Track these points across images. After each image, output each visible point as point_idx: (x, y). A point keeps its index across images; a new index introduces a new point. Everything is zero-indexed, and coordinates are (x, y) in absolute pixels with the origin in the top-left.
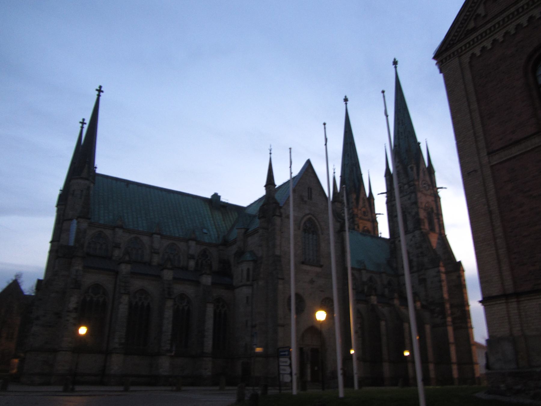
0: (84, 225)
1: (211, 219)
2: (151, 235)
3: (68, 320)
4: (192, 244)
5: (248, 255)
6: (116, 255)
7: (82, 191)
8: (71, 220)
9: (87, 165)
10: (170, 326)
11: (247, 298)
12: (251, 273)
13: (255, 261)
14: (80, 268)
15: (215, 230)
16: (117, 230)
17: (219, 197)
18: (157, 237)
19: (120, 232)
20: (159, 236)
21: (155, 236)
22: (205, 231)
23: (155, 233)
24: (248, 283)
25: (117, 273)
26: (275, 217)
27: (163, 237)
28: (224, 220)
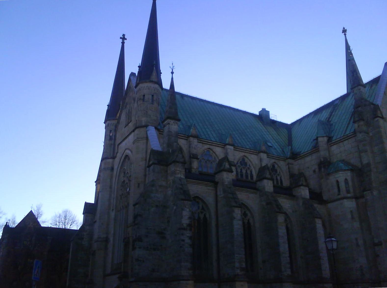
0: (174, 127)
1: (268, 133)
2: (224, 145)
3: (183, 241)
4: (264, 156)
5: (341, 165)
6: (195, 167)
7: (153, 96)
8: (146, 126)
9: (154, 68)
10: (287, 246)
11: (351, 212)
12: (350, 184)
13: (352, 170)
14: (183, 177)
15: (276, 144)
16: (191, 139)
17: (268, 112)
18: (230, 148)
19: (195, 142)
20: (232, 148)
21: (228, 147)
22: (269, 144)
23: (229, 144)
24: (349, 195)
25: (216, 184)
26: (376, 119)
27: (236, 148)
28: (278, 135)
